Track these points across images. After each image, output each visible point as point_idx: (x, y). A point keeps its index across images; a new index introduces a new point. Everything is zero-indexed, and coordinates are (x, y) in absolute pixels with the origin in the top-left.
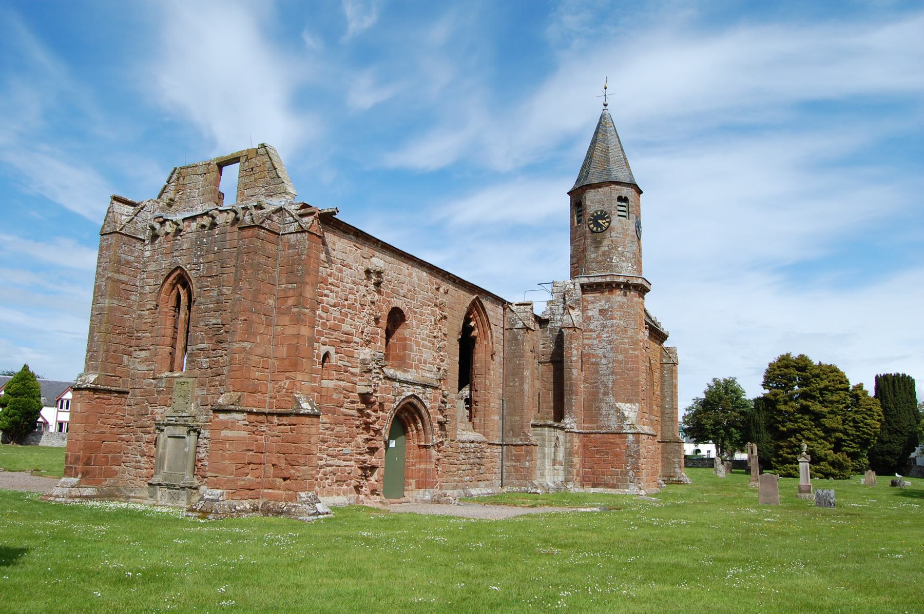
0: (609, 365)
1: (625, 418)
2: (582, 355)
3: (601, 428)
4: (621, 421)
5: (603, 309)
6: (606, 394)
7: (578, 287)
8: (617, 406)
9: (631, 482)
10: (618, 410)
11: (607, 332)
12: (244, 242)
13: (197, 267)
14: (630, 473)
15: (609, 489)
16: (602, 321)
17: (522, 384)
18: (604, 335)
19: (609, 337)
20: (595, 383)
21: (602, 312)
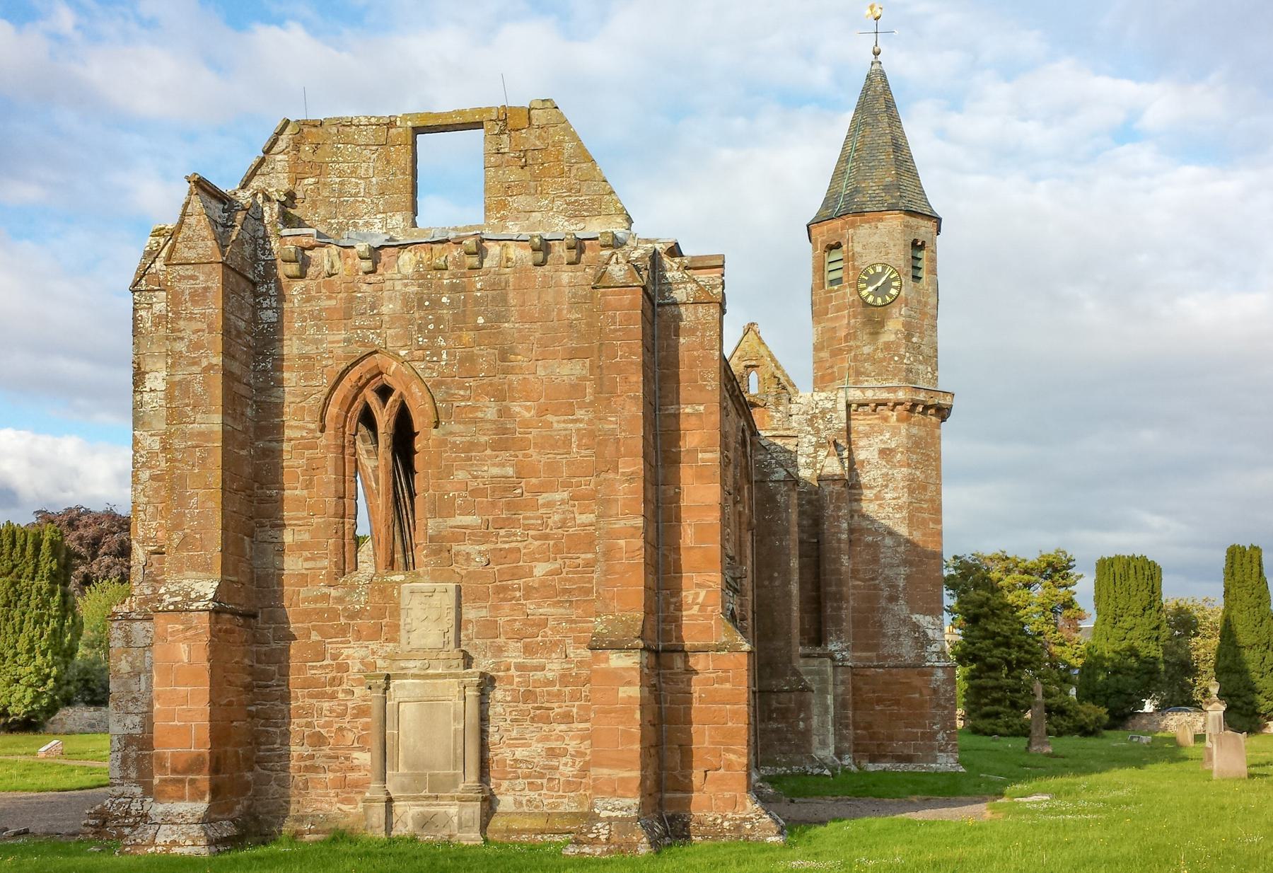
0: (899, 549)
1: (930, 642)
2: (851, 531)
3: (885, 658)
4: (922, 647)
5: (888, 449)
6: (893, 599)
7: (842, 406)
8: (914, 620)
9: (941, 751)
10: (916, 627)
11: (895, 489)
12: (614, 317)
13: (432, 355)
14: (940, 736)
15: (902, 765)
16: (884, 470)
17: (787, 583)
18: (888, 496)
19: (899, 498)
20: (873, 579)
21: (885, 453)
